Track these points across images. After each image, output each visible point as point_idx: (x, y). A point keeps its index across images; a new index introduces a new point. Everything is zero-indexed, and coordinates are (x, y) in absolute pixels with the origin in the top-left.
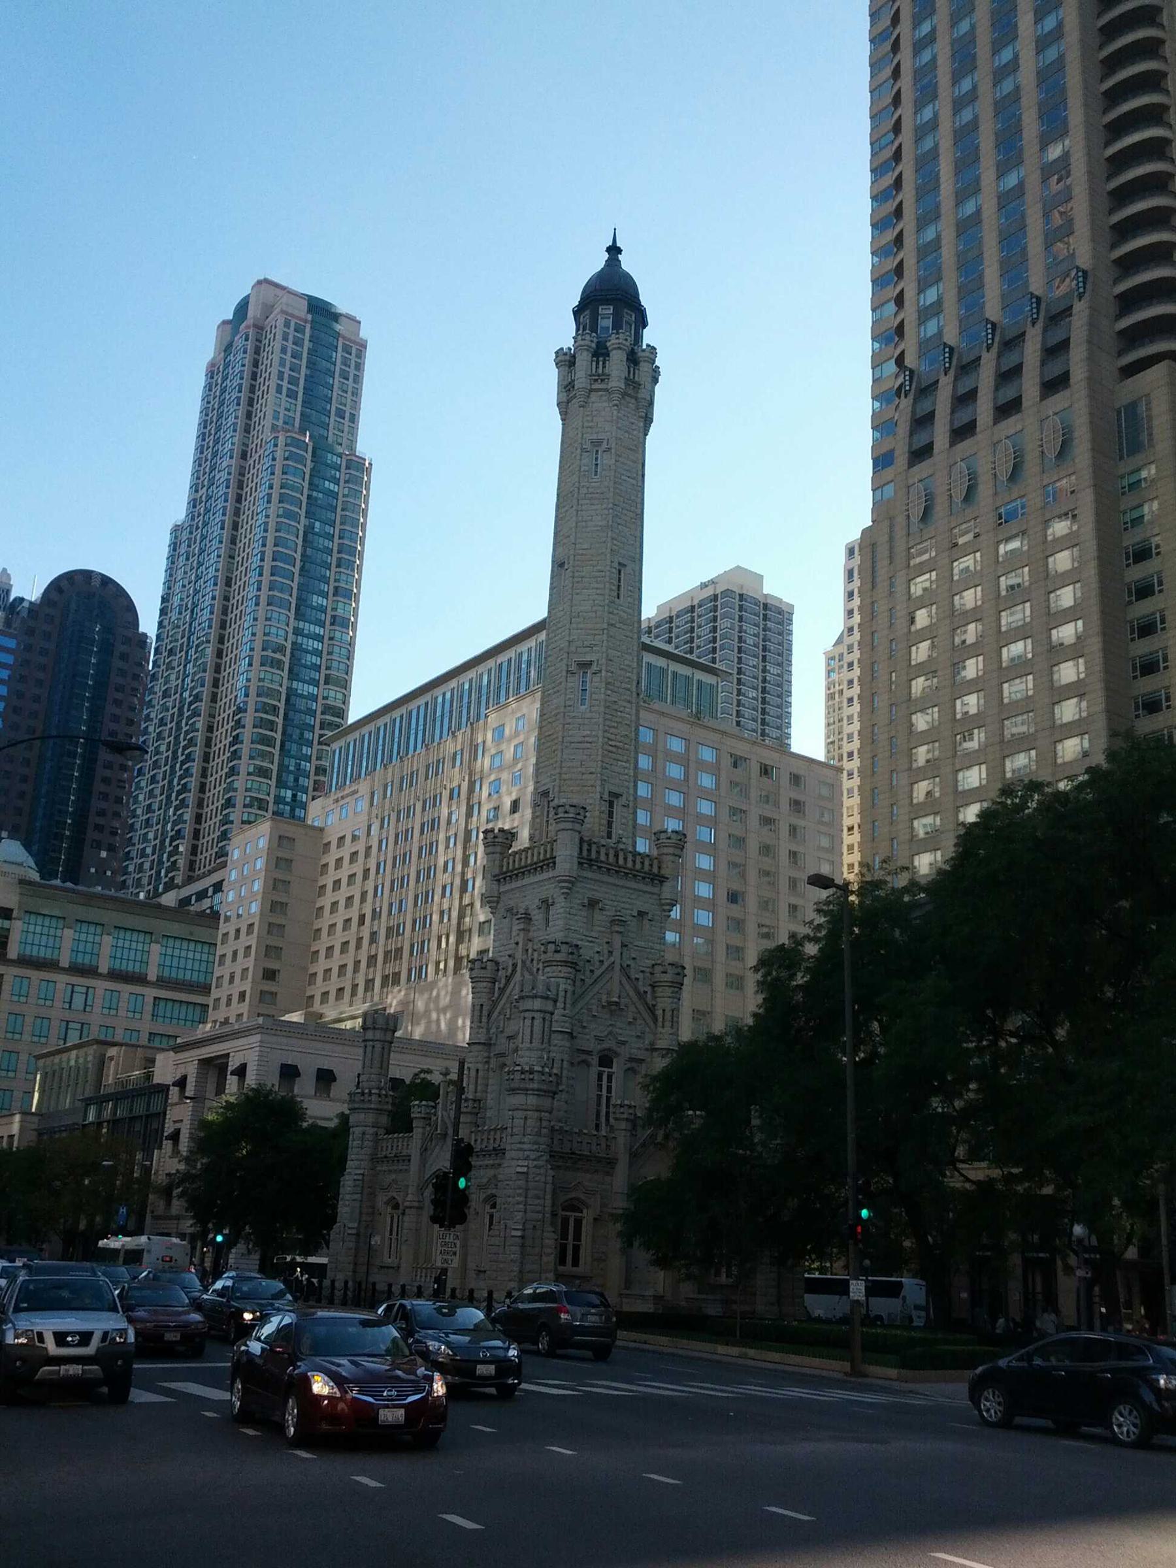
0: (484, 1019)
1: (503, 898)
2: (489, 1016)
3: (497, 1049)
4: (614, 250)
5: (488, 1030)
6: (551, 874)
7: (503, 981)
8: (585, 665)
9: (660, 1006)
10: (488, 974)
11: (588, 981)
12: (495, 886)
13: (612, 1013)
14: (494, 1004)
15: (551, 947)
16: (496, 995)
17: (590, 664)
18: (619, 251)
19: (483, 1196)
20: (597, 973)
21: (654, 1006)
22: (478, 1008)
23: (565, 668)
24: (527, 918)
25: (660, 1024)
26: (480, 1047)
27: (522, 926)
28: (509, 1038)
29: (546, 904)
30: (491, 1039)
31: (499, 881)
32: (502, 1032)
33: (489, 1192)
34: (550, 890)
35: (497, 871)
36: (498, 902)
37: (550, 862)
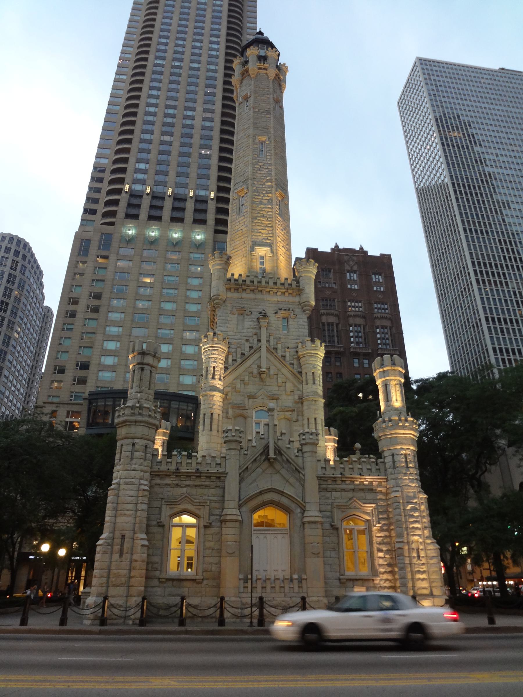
9: (304, 372)
11: (239, 361)
13: (262, 379)
20: (247, 354)
21: (300, 373)
25: (304, 383)
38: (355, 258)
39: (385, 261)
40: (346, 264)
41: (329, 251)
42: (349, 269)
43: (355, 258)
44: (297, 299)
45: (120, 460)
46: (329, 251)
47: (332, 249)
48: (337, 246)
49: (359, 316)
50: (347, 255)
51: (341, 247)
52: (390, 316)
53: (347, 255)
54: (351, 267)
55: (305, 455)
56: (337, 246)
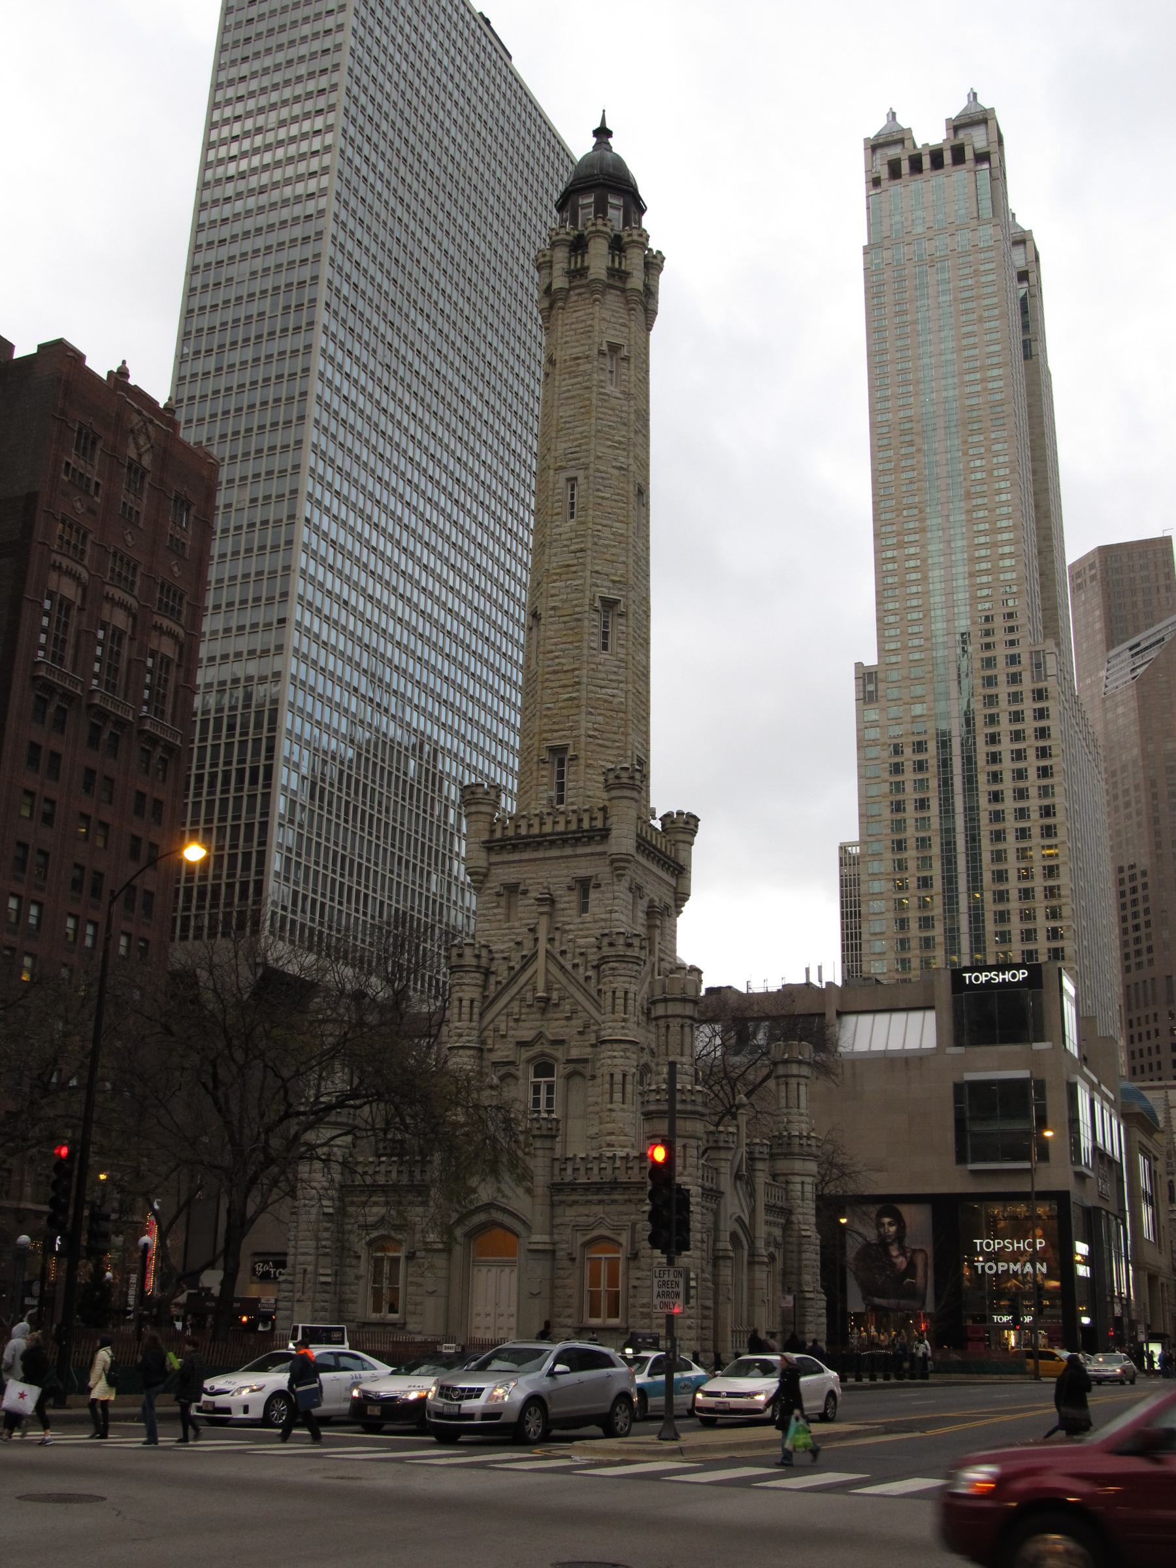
0: (476, 1017)
1: (494, 871)
2: (481, 1015)
3: (496, 1057)
4: (603, 133)
5: (482, 1031)
6: (599, 849)
7: (503, 975)
8: (609, 604)
10: (484, 962)
12: (483, 855)
14: (488, 1003)
15: (621, 940)
16: (492, 988)
17: (617, 602)
18: (609, 134)
19: (581, 1239)
22: (466, 1003)
23: (587, 601)
24: (549, 901)
26: (471, 1052)
27: (546, 909)
28: (521, 1044)
29: (584, 886)
30: (483, 1042)
31: (489, 850)
32: (503, 1036)
33: (595, 1233)
34: (599, 869)
35: (485, 837)
36: (486, 875)
37: (604, 834)
38: (150, 428)
39: (205, 473)
40: (130, 440)
41: (104, 376)
42: (134, 457)
43: (150, 428)
44: (673, 882)
45: (684, 1167)
46: (104, 376)
47: (110, 373)
48: (123, 373)
49: (127, 608)
50: (140, 413)
51: (132, 381)
52: (181, 633)
53: (140, 413)
54: (140, 455)
55: (758, 1174)
56: (123, 373)
